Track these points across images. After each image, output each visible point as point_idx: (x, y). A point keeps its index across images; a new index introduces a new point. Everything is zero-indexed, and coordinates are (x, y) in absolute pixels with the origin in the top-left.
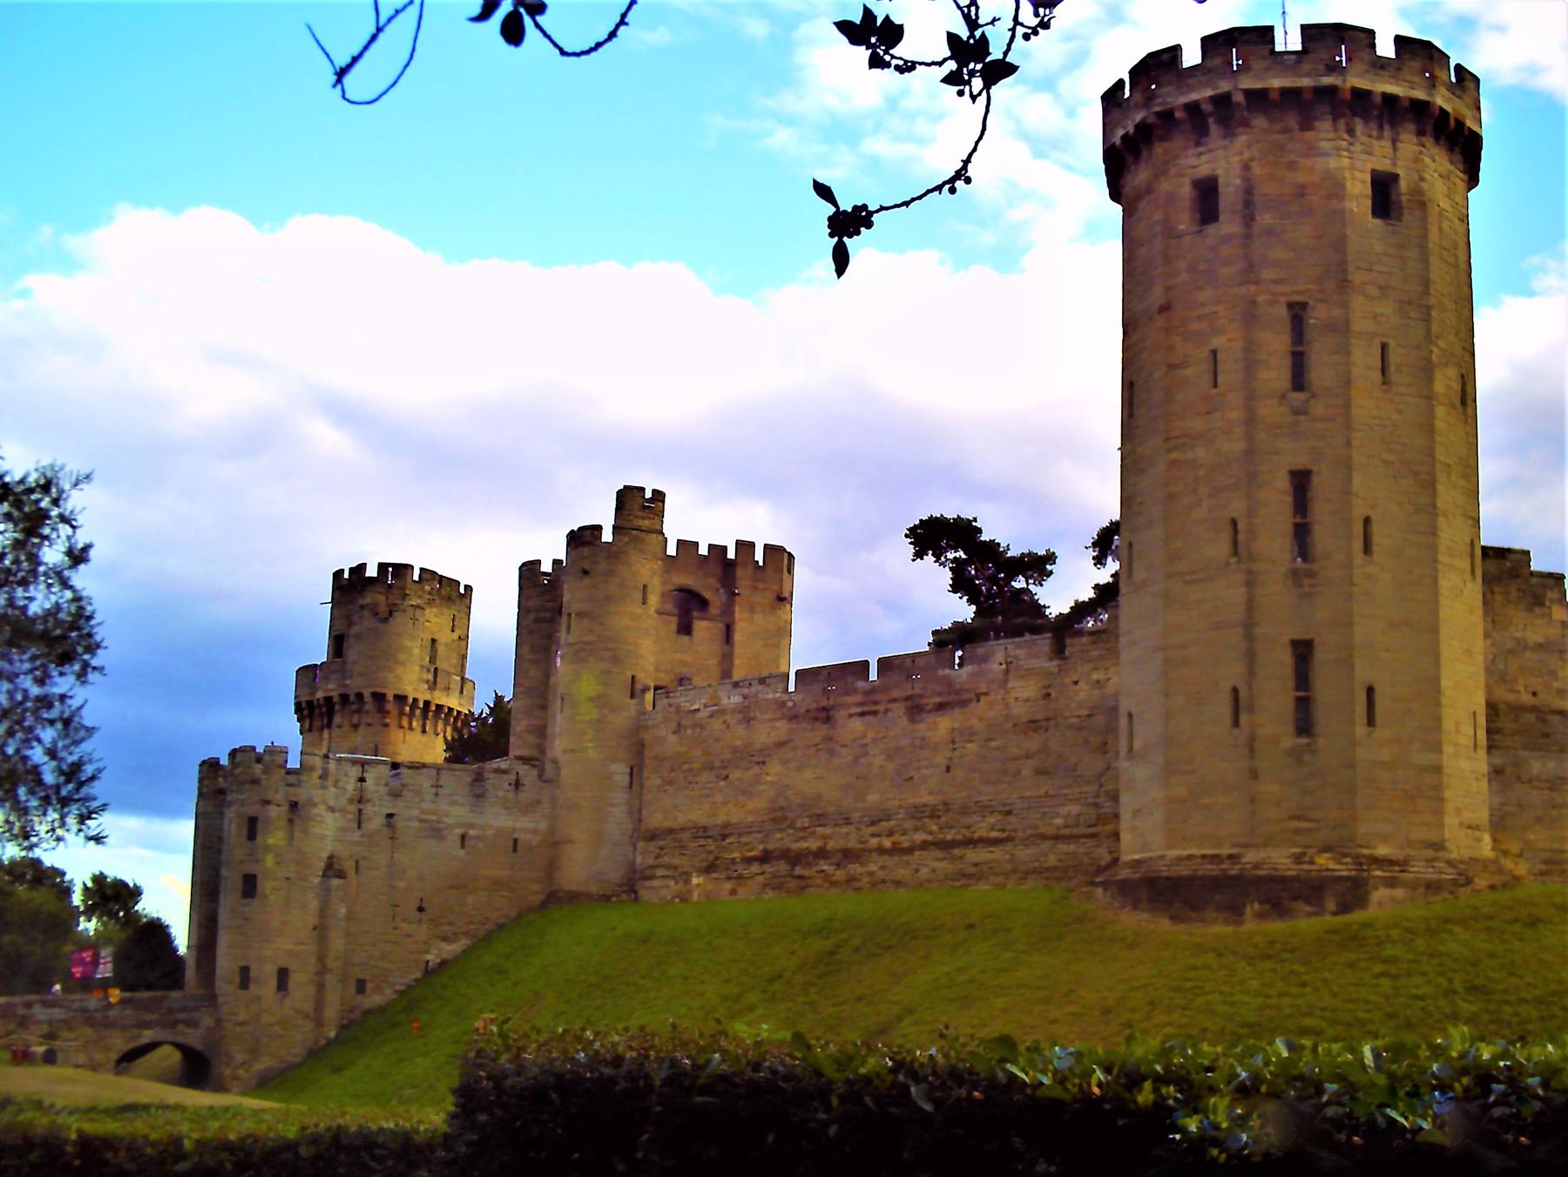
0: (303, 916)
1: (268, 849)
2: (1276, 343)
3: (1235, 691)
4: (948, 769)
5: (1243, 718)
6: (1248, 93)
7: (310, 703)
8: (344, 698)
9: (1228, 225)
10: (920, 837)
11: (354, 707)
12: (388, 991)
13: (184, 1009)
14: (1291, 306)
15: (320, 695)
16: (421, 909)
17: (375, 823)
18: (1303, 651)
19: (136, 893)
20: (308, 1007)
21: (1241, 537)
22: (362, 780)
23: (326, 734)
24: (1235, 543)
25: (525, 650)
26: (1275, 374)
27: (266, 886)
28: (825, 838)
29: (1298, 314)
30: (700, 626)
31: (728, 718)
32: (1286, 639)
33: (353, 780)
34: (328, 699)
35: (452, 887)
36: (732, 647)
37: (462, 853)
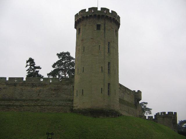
2: (107, 46)
3: (102, 89)
4: (39, 95)
5: (103, 92)
6: (106, 16)
9: (102, 30)
10: (33, 104)
14: (109, 42)
18: (109, 84)
19: (135, 91)
21: (103, 69)
24: (102, 70)
26: (107, 50)
28: (13, 103)
29: (109, 43)
32: (108, 83)
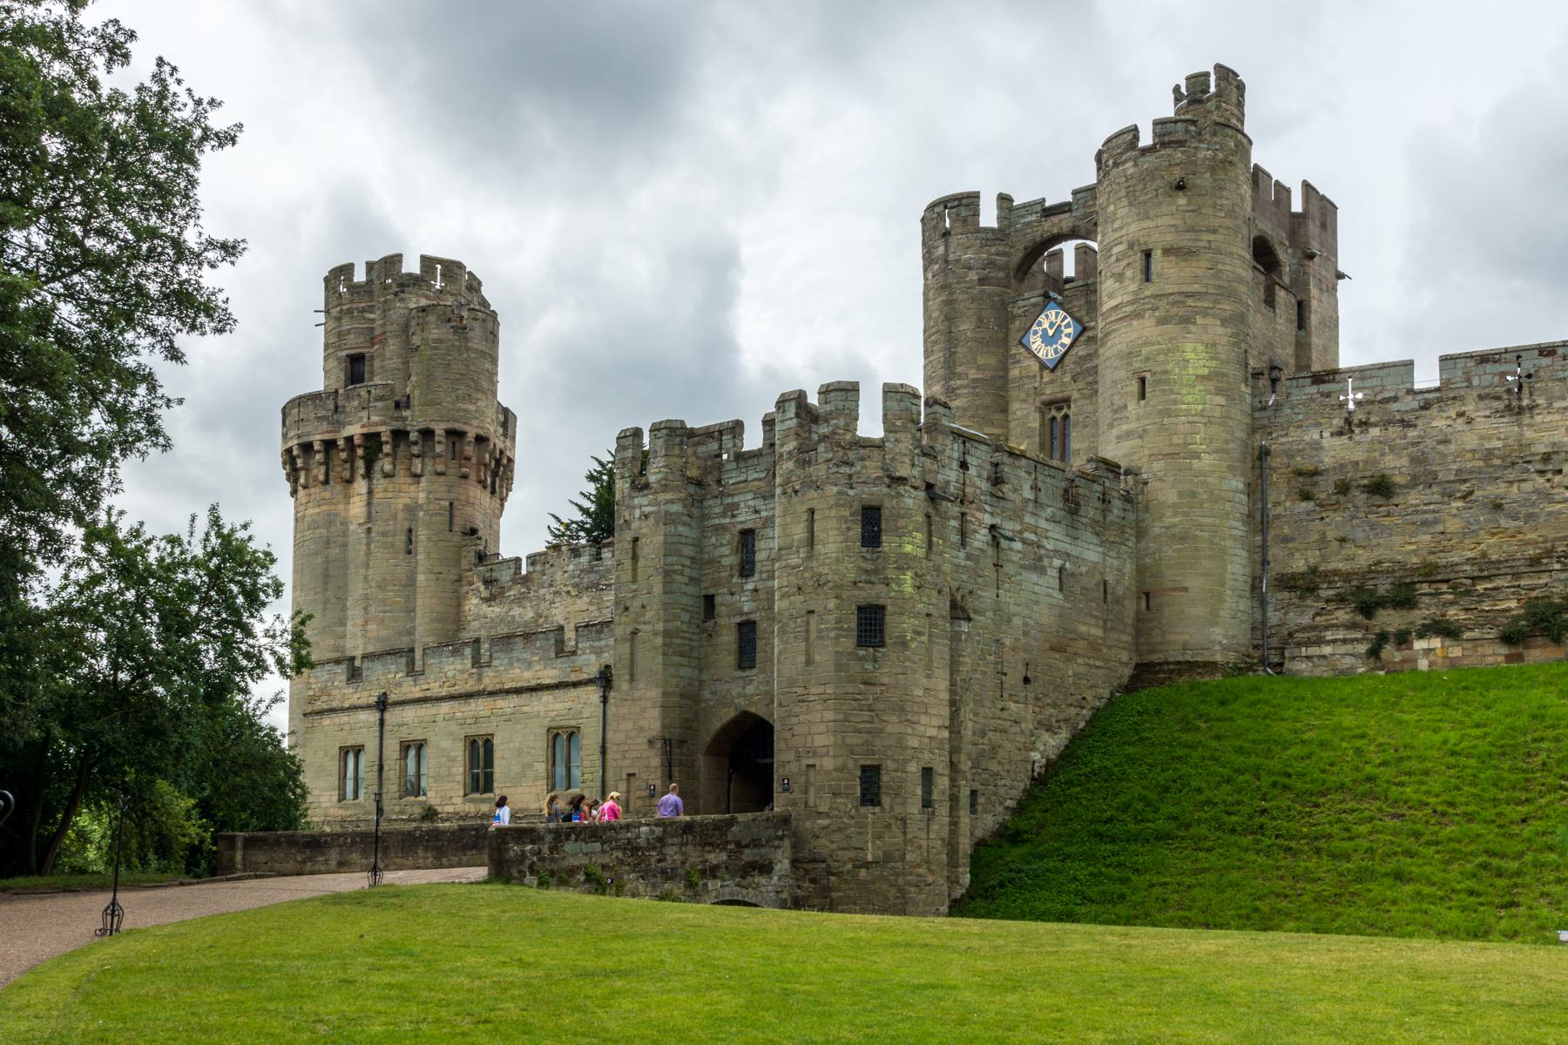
0: (941, 685)
1: (904, 563)
7: (330, 445)
8: (399, 435)
11: (415, 450)
12: (1000, 809)
13: (756, 843)
15: (355, 430)
16: (1026, 680)
17: (980, 539)
20: (945, 833)
22: (964, 465)
23: (360, 486)
25: (966, 327)
27: (900, 625)
30: (1281, 294)
31: (1470, 408)
33: (955, 465)
34: (372, 440)
35: (1052, 649)
36: (1309, 334)
37: (1060, 596)
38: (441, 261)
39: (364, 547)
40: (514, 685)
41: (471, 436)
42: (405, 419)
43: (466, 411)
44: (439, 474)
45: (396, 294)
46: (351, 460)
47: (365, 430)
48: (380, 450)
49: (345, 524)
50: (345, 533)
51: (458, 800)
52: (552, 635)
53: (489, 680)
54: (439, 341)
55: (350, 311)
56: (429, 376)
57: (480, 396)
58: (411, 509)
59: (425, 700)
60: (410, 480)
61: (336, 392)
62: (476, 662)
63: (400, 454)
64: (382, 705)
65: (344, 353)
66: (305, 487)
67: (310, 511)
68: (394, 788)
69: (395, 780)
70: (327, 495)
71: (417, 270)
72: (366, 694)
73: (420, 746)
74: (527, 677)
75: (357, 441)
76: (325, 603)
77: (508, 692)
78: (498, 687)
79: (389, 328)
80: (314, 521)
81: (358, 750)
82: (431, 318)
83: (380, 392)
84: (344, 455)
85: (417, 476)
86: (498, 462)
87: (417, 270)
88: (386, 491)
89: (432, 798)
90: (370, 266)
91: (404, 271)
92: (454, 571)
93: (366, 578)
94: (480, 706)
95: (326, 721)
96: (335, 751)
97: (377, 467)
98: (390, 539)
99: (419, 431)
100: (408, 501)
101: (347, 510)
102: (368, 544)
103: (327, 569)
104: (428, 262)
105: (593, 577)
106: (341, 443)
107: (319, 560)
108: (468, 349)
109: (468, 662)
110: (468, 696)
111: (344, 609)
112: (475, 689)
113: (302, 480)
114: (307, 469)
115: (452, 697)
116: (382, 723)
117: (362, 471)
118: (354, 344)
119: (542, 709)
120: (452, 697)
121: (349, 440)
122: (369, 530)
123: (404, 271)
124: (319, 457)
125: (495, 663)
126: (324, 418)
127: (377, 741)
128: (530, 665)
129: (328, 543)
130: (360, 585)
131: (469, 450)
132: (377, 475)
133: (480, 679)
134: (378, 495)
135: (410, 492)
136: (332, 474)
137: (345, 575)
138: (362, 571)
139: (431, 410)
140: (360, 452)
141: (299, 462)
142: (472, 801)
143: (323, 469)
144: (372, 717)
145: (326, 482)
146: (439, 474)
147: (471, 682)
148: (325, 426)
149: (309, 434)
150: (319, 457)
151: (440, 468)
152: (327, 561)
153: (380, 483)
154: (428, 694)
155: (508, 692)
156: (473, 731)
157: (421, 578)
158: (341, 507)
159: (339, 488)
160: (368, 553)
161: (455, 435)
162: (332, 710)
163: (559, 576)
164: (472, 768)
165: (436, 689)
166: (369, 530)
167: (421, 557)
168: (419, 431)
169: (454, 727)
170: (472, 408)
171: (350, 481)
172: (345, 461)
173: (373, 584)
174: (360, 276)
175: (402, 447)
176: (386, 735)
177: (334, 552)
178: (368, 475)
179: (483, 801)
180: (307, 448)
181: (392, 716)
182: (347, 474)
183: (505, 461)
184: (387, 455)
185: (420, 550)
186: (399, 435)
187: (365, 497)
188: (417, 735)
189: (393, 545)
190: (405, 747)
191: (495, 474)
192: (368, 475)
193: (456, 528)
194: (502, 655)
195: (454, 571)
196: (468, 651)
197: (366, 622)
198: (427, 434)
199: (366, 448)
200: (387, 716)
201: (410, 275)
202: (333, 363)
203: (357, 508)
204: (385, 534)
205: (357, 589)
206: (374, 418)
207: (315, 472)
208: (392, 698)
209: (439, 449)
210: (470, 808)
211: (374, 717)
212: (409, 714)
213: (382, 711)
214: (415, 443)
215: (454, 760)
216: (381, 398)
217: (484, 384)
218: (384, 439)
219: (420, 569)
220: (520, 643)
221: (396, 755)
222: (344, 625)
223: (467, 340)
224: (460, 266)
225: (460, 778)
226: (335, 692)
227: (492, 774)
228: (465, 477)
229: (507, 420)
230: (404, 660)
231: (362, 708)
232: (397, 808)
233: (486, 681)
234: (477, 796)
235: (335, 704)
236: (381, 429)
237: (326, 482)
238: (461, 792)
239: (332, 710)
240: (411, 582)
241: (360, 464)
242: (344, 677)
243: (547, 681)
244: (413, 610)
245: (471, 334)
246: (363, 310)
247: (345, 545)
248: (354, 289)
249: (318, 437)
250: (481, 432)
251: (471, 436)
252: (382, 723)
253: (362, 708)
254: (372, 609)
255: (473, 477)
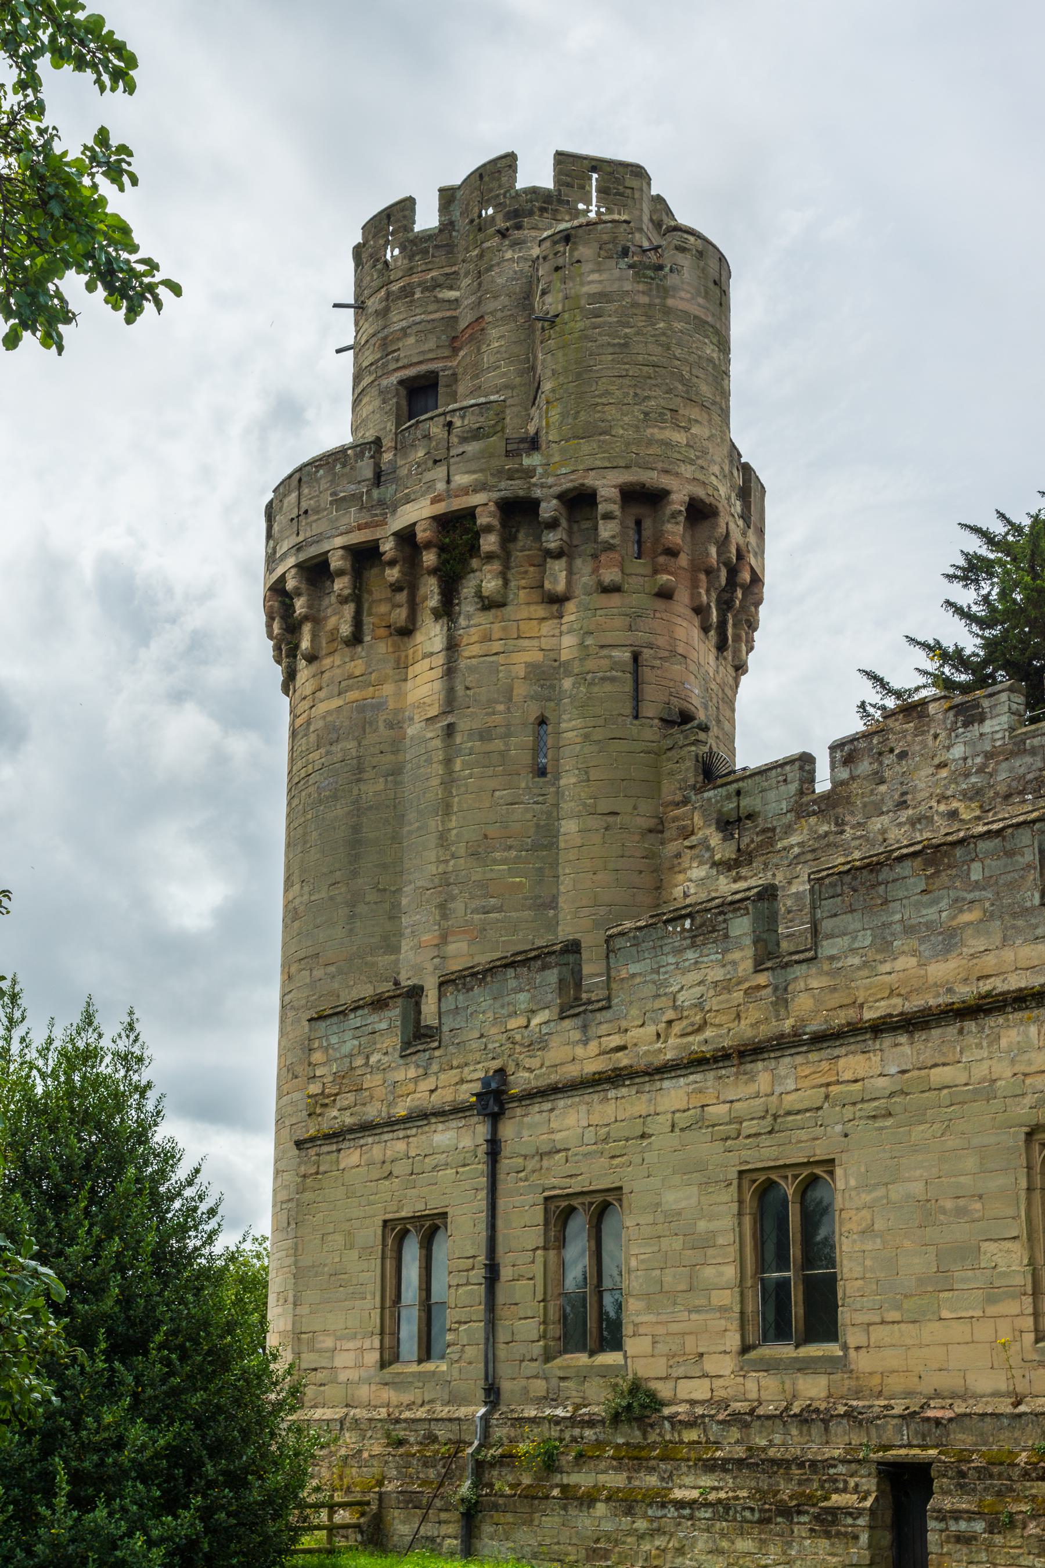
7: (364, 557)
8: (518, 511)
11: (552, 540)
15: (417, 512)
23: (431, 636)
34: (456, 527)
38: (596, 164)
39: (439, 769)
40: (896, 1006)
41: (678, 500)
42: (529, 473)
43: (667, 444)
44: (607, 590)
45: (503, 234)
46: (409, 585)
47: (441, 508)
48: (474, 549)
49: (396, 724)
50: (396, 745)
51: (724, 1365)
52: (1025, 837)
53: (811, 1001)
54: (603, 296)
55: (406, 292)
56: (581, 374)
57: (695, 413)
58: (545, 675)
59: (615, 1078)
60: (540, 611)
61: (378, 442)
62: (768, 956)
63: (518, 556)
64: (495, 1101)
65: (394, 379)
66: (312, 658)
67: (322, 708)
68: (530, 1328)
69: (532, 1306)
70: (358, 667)
71: (546, 180)
72: (453, 1075)
73: (603, 1206)
74: (946, 977)
75: (422, 535)
76: (352, 905)
77: (880, 1028)
78: (840, 1019)
79: (490, 306)
80: (331, 728)
81: (431, 1227)
82: (585, 251)
83: (472, 420)
84: (393, 574)
85: (556, 600)
86: (733, 572)
87: (546, 180)
88: (487, 638)
89: (640, 1355)
90: (447, 196)
91: (520, 185)
92: (645, 807)
93: (443, 838)
94: (788, 1081)
95: (351, 1157)
96: (371, 1233)
97: (467, 590)
98: (498, 745)
99: (560, 497)
100: (536, 657)
101: (400, 695)
102: (448, 762)
103: (356, 829)
104: (569, 165)
105: (1023, 764)
106: (388, 547)
107: (340, 809)
108: (667, 311)
109: (743, 958)
110: (749, 1053)
111: (394, 914)
112: (765, 1031)
113: (305, 644)
114: (315, 618)
115: (698, 1063)
116: (494, 1149)
117: (433, 602)
118: (415, 354)
119: (1003, 1070)
120: (698, 1063)
121: (406, 537)
122: (450, 730)
123: (520, 185)
124: (341, 585)
125: (828, 948)
126: (355, 498)
127: (481, 1200)
128: (949, 940)
129: (360, 769)
130: (432, 855)
131: (675, 532)
132: (467, 606)
133: (782, 999)
134: (471, 650)
135: (538, 638)
136: (368, 620)
137: (396, 838)
138: (434, 824)
139: (586, 447)
140: (429, 558)
141: (300, 605)
142: (769, 1366)
143: (349, 610)
144: (465, 1138)
145: (356, 639)
146: (607, 590)
147: (753, 1014)
148: (352, 516)
149: (319, 539)
150: (341, 585)
151: (610, 575)
152: (358, 810)
153: (473, 623)
154: (623, 1060)
155: (880, 1028)
156: (766, 1153)
157: (569, 827)
158: (388, 689)
159: (382, 648)
160: (449, 780)
161: (644, 499)
162: (366, 1128)
163: (923, 779)
164: (762, 1266)
165: (645, 1041)
166: (450, 730)
167: (568, 780)
168: (560, 497)
169: (704, 1147)
170: (679, 437)
171: (406, 632)
172: (396, 588)
173: (461, 849)
174: (427, 218)
175: (523, 538)
176: (507, 1182)
177: (373, 788)
178: (447, 610)
179: (805, 1366)
180: (316, 572)
181: (523, 1131)
182: (400, 616)
183: (746, 576)
184: (490, 557)
185: (567, 763)
186: (518, 511)
187: (440, 660)
188: (595, 1175)
189: (503, 754)
190: (559, 1213)
191: (725, 605)
192: (447, 610)
193: (649, 710)
194: (851, 921)
195: (645, 807)
196: (741, 926)
197: (444, 938)
198: (580, 502)
199: (442, 549)
200: (507, 1130)
201: (534, 191)
202: (371, 404)
203: (424, 686)
204: (484, 735)
205: (423, 866)
206: (461, 479)
207: (332, 622)
208: (521, 1080)
209: (607, 531)
210: (765, 1390)
211: (471, 1136)
212: (570, 1121)
213: (495, 1118)
214: (553, 525)
215: (705, 1244)
216: (476, 434)
217: (705, 389)
218: (482, 520)
219: (566, 806)
220: (912, 878)
221: (534, 1237)
222: (396, 950)
223: (665, 292)
224: (638, 172)
225: (727, 1298)
226: (371, 1081)
227: (831, 1281)
228: (665, 594)
229: (749, 488)
230: (552, 976)
231: (441, 1114)
232: (539, 1387)
233: (802, 1004)
234: (785, 1351)
235: (373, 1112)
236: (477, 499)
237: (356, 639)
238: (733, 1341)
239: (366, 1128)
240: (545, 840)
241: (431, 591)
242: (393, 1041)
243: (1015, 982)
244: (553, 903)
245: (672, 280)
246: (436, 285)
247: (396, 772)
248: (417, 246)
249: (339, 541)
250: (700, 492)
251: (678, 500)
252: (494, 1149)
253: (441, 1114)
254: (458, 906)
255: (683, 596)
